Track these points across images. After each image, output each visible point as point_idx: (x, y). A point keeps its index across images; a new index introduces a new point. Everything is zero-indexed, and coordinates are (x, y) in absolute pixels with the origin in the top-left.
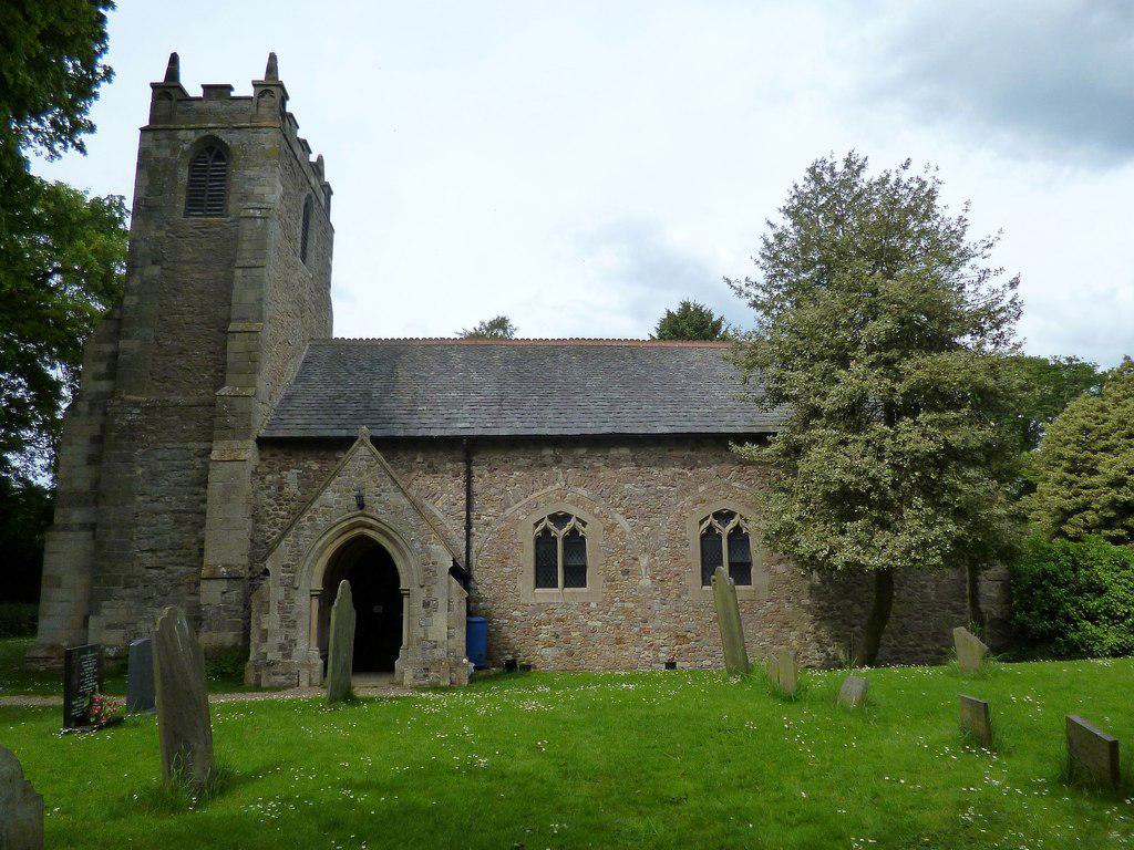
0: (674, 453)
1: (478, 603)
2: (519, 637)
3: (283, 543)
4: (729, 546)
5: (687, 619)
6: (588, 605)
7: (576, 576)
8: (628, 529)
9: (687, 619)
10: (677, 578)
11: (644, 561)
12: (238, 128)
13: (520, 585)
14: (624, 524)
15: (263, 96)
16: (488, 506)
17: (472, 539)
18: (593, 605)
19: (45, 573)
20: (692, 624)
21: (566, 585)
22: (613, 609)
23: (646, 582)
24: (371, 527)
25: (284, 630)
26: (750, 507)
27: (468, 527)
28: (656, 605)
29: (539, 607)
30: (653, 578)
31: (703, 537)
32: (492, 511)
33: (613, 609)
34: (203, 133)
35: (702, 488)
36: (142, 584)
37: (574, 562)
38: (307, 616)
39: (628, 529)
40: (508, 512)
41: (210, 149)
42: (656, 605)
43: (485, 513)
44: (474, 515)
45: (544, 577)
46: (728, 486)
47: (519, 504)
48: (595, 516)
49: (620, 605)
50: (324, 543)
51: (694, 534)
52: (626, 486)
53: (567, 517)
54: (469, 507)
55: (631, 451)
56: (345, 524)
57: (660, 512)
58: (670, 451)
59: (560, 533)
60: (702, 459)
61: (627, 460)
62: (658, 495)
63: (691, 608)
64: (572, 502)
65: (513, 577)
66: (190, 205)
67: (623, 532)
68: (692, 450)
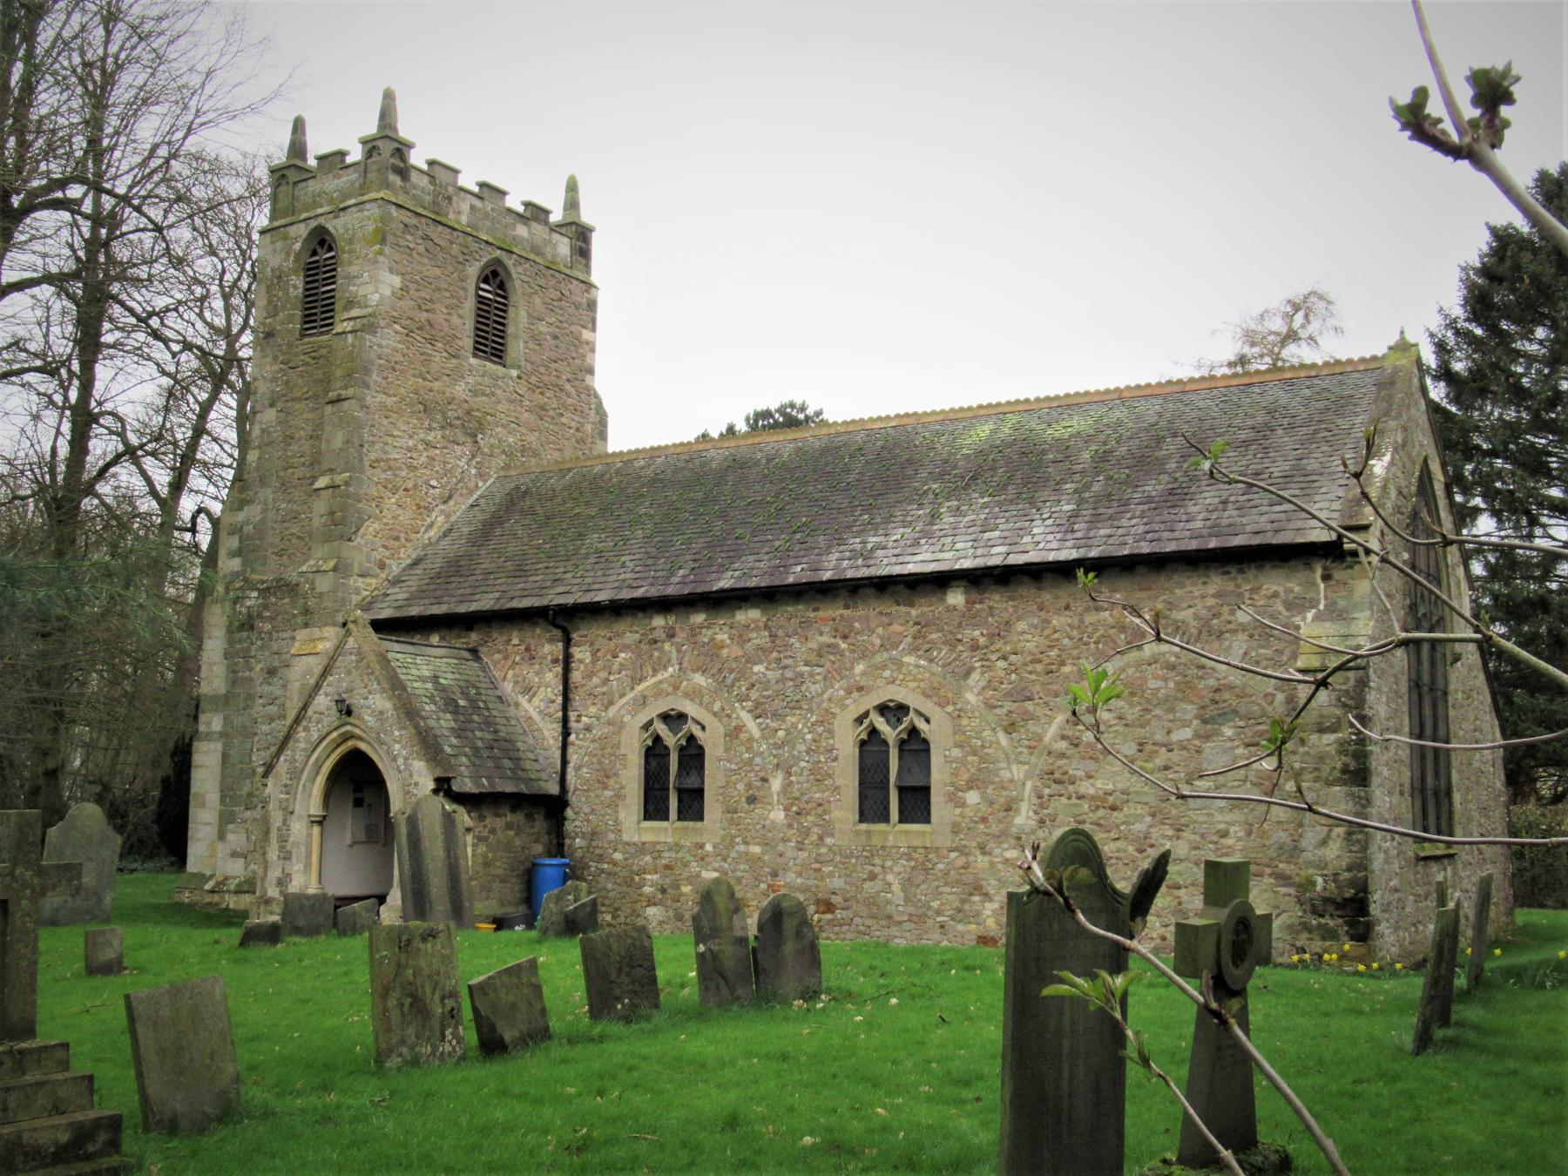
0: (821, 614)
1: (574, 839)
2: (619, 889)
3: (282, 758)
4: (680, 763)
5: (831, 875)
6: (702, 846)
7: (692, 803)
8: (756, 734)
9: (831, 875)
10: (820, 810)
11: (776, 784)
12: (344, 209)
13: (622, 815)
14: (752, 727)
15: (370, 156)
16: (589, 702)
17: (570, 750)
18: (709, 848)
19: (192, 791)
20: (837, 883)
21: (903, 819)
22: (733, 854)
23: (778, 815)
24: (360, 739)
25: (281, 863)
26: (927, 696)
27: (566, 733)
28: (789, 849)
29: (642, 848)
30: (786, 809)
31: (863, 743)
32: (593, 710)
33: (733, 854)
34: (313, 224)
35: (859, 668)
36: (260, 805)
37: (691, 782)
38: (303, 848)
39: (756, 734)
40: (612, 711)
41: (322, 243)
42: (789, 849)
43: (586, 713)
44: (572, 716)
45: (654, 808)
46: (899, 665)
47: (624, 700)
48: (715, 714)
49: (742, 848)
50: (317, 760)
51: (846, 740)
52: (756, 669)
53: (682, 717)
54: (565, 709)
55: (764, 612)
56: (335, 735)
57: (800, 708)
58: (815, 610)
59: (670, 740)
60: (859, 620)
61: (757, 629)
62: (799, 680)
63: (838, 858)
64: (686, 695)
65: (613, 805)
66: (306, 323)
67: (751, 739)
68: (846, 607)
